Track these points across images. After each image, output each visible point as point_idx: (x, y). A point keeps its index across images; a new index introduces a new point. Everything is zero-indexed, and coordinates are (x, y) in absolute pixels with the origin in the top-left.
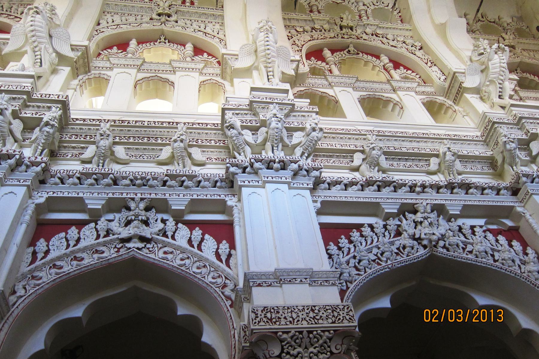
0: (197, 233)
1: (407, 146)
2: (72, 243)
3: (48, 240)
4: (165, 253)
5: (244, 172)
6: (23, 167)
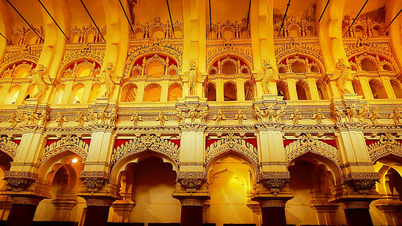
0: (85, 143)
1: (149, 112)
2: (55, 146)
3: (49, 146)
4: (76, 149)
5: (93, 128)
6: (39, 129)
